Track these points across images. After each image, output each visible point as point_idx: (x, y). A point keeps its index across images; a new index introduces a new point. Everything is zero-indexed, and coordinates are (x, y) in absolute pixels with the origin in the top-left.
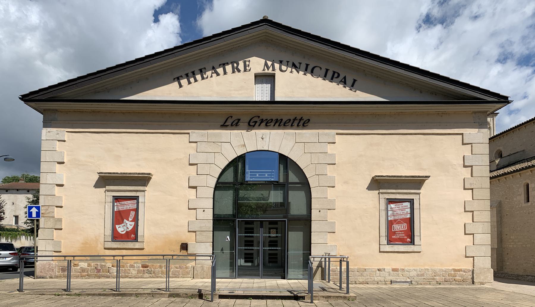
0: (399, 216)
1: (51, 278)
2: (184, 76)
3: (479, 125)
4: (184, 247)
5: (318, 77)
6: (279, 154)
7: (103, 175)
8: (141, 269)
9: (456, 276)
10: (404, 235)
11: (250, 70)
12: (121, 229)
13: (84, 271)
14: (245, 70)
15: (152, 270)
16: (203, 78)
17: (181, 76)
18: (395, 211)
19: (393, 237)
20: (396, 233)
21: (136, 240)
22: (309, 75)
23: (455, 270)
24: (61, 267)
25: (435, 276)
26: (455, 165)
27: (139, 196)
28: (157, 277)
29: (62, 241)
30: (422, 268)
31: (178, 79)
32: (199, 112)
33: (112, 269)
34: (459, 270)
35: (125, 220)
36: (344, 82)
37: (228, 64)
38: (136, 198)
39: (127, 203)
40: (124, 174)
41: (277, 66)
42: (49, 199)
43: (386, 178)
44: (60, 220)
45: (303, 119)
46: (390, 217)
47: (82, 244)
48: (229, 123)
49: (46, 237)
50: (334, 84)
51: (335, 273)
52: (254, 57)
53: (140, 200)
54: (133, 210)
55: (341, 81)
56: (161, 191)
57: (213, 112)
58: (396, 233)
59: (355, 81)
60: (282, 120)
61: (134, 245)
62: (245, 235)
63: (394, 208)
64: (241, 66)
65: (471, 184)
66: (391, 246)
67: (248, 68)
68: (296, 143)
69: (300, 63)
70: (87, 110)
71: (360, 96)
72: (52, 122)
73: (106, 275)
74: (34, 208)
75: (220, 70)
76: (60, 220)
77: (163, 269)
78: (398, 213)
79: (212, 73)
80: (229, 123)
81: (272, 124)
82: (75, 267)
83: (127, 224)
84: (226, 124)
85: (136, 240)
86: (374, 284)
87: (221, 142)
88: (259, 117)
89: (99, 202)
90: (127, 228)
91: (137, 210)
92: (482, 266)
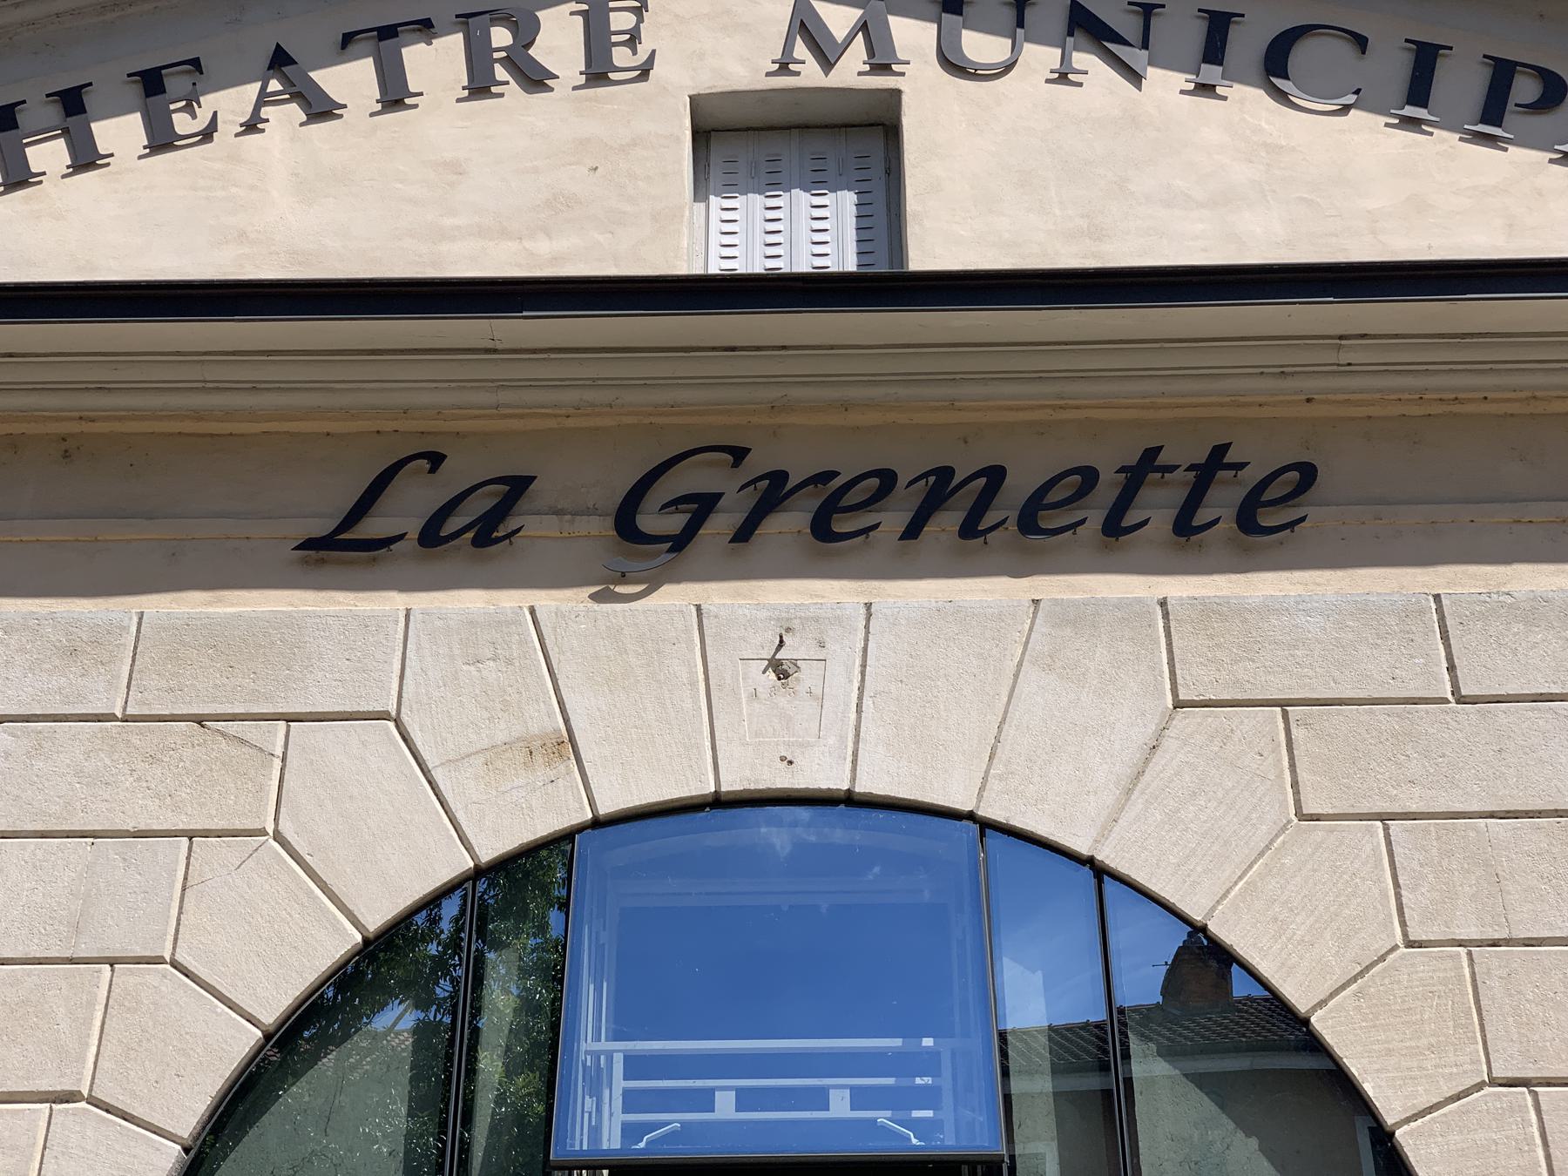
5: (1345, 109)
11: (644, 72)
14: (598, 73)
16: (161, 141)
32: (75, 428)
37: (426, 28)
45: (1240, 466)
57: (229, 415)
60: (995, 475)
67: (621, 56)
68: (1179, 705)
79: (263, 99)
81: (893, 519)
84: (372, 527)
87: (290, 719)
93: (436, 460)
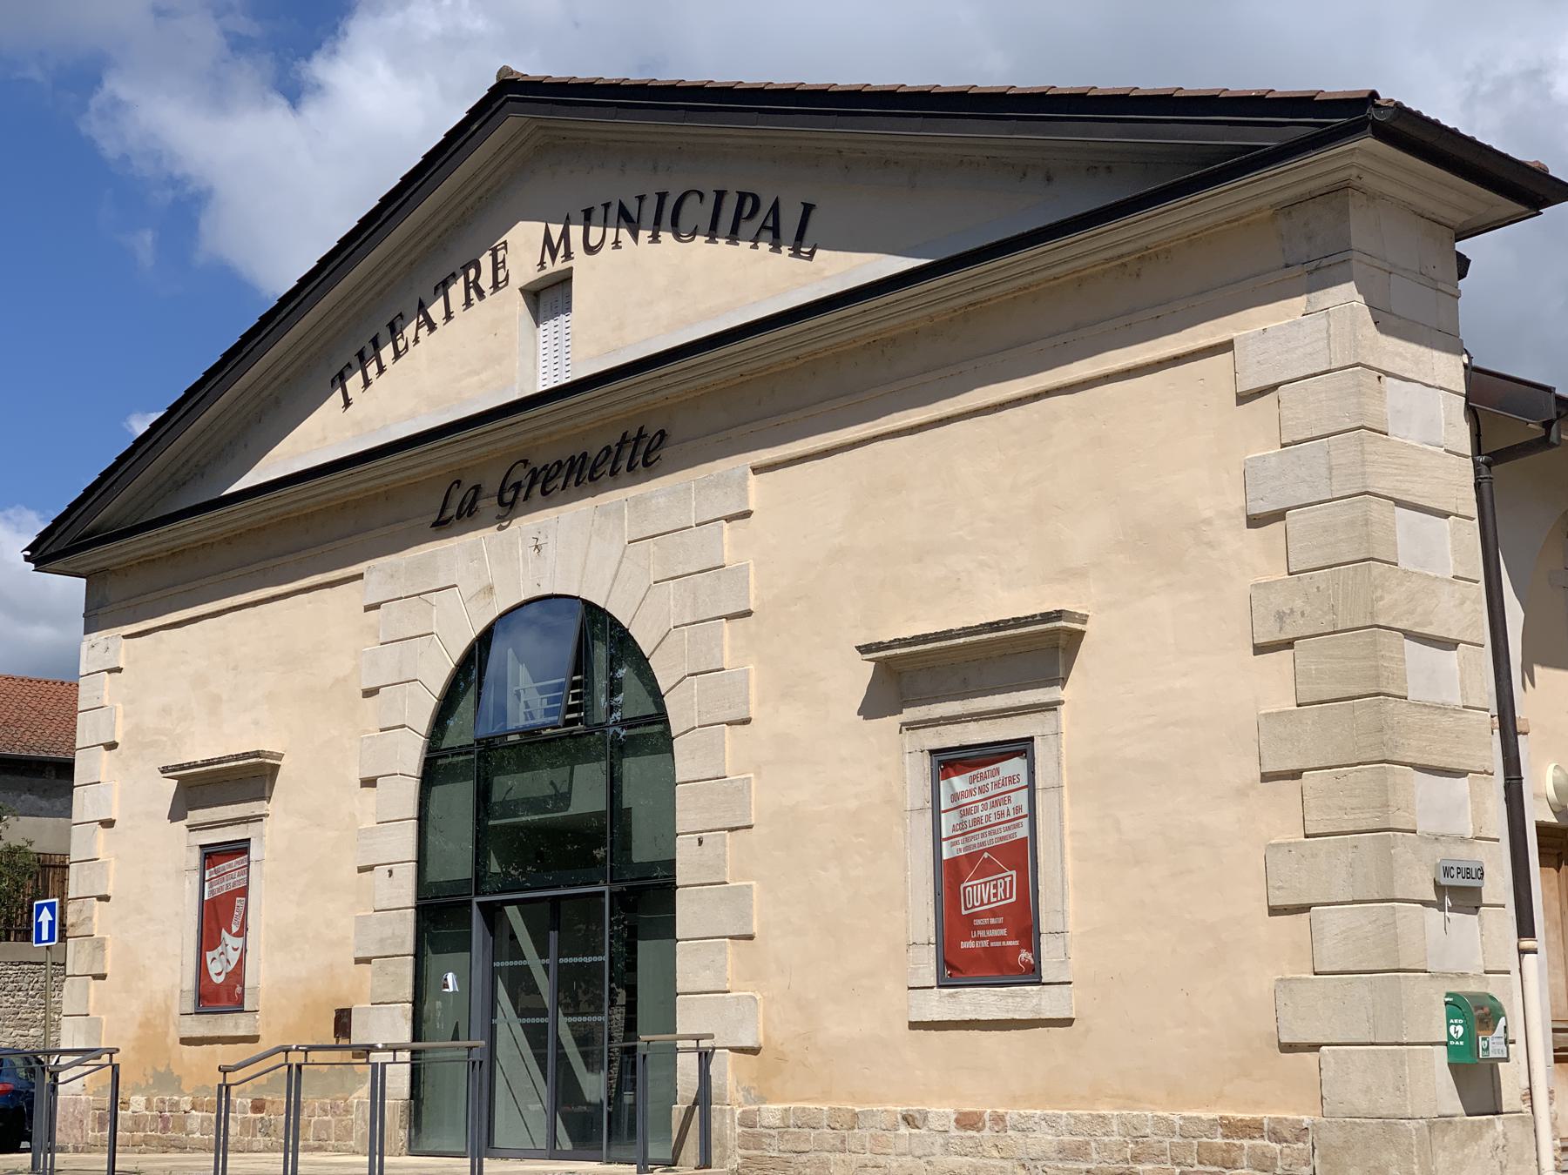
0: (983, 835)
3: (1310, 273)
4: (343, 1022)
6: (582, 599)
8: (250, 1115)
9: (1234, 1162)
10: (1003, 932)
18: (969, 812)
19: (964, 945)
20: (978, 922)
23: (1234, 1129)
24: (97, 1112)
25: (1136, 1158)
26: (1208, 522)
27: (1031, 739)
29: (103, 1017)
30: (1078, 1112)
34: (1251, 1129)
38: (1022, 748)
39: (230, 866)
43: (898, 651)
46: (953, 845)
47: (141, 1026)
50: (745, 246)
51: (753, 1135)
55: (763, 227)
58: (978, 922)
59: (808, 208)
60: (585, 455)
61: (236, 1026)
62: (511, 963)
63: (963, 795)
65: (1281, 617)
66: (950, 995)
69: (641, 198)
71: (827, 273)
73: (179, 1139)
78: (978, 820)
83: (227, 945)
84: (443, 518)
85: (237, 1006)
92: (1363, 1105)
93: (458, 482)
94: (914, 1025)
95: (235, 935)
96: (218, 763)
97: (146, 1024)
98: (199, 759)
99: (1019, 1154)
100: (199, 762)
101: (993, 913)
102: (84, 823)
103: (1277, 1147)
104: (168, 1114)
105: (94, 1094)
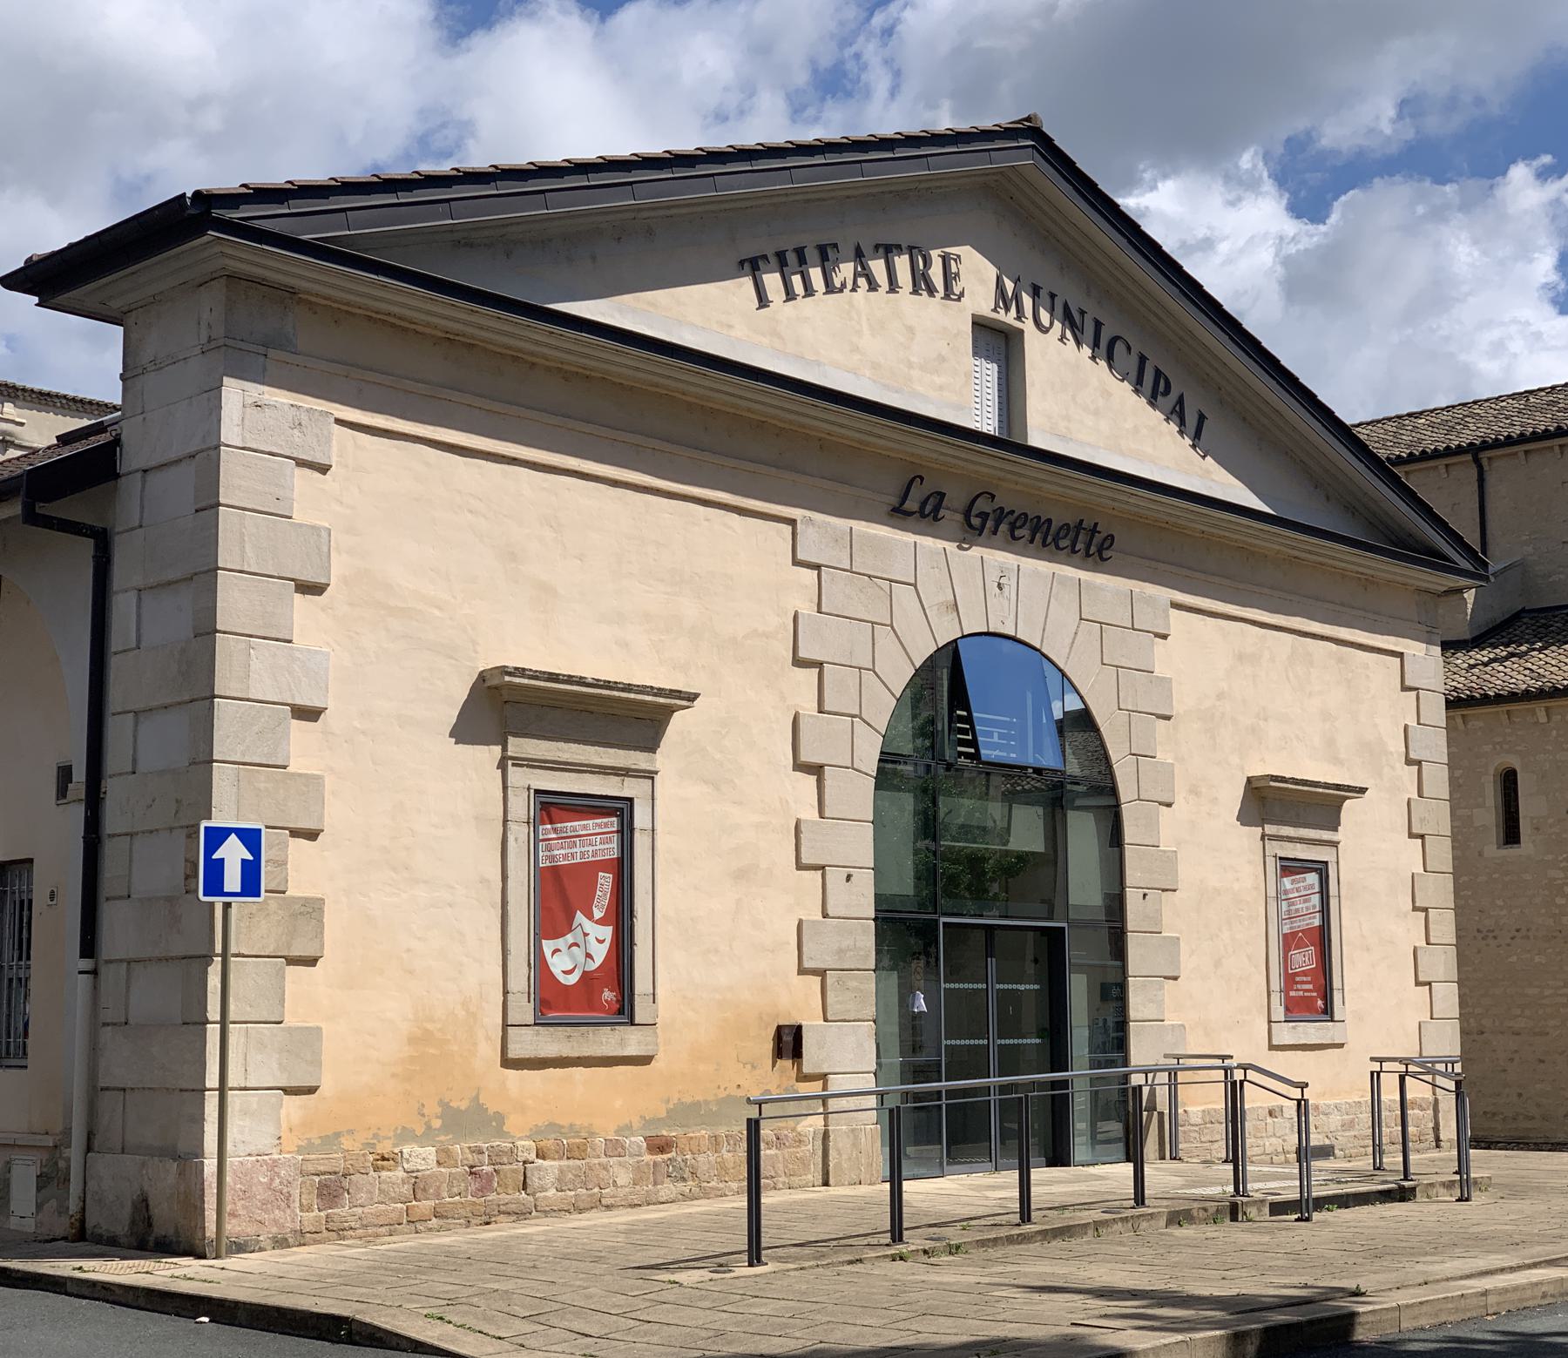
1: (280, 1243)
2: (773, 260)
5: (1122, 381)
7: (526, 681)
8: (648, 1158)
10: (1310, 987)
12: (564, 963)
13: (424, 1190)
15: (685, 1161)
16: (830, 288)
17: (765, 257)
18: (1293, 904)
20: (1298, 979)
21: (624, 1011)
22: (1103, 364)
24: (317, 1179)
28: (706, 1195)
31: (753, 266)
32: (823, 435)
33: (539, 1169)
35: (580, 917)
36: (1177, 413)
37: (899, 249)
39: (585, 827)
40: (608, 685)
41: (1027, 301)
42: (262, 786)
44: (313, 909)
45: (1099, 532)
47: (413, 1040)
48: (912, 504)
49: (248, 1009)
52: (968, 247)
53: (641, 818)
54: (603, 865)
56: (706, 782)
58: (1298, 979)
60: (1049, 521)
61: (622, 1044)
64: (936, 274)
66: (1294, 1028)
70: (428, 325)
71: (1214, 477)
72: (272, 353)
74: (233, 836)
75: (878, 267)
76: (313, 909)
77: (724, 1151)
78: (1297, 910)
80: (912, 504)
81: (1024, 532)
82: (384, 1174)
83: (586, 935)
86: (1262, 1163)
88: (993, 497)
89: (476, 818)
90: (589, 956)
91: (623, 869)
94: (1341, 1046)
95: (599, 922)
96: (623, 690)
97: (420, 1038)
98: (589, 673)
99: (1326, 1129)
100: (590, 681)
101: (1304, 973)
102: (248, 700)
103: (1421, 1113)
104: (487, 1169)
105: (300, 1151)
